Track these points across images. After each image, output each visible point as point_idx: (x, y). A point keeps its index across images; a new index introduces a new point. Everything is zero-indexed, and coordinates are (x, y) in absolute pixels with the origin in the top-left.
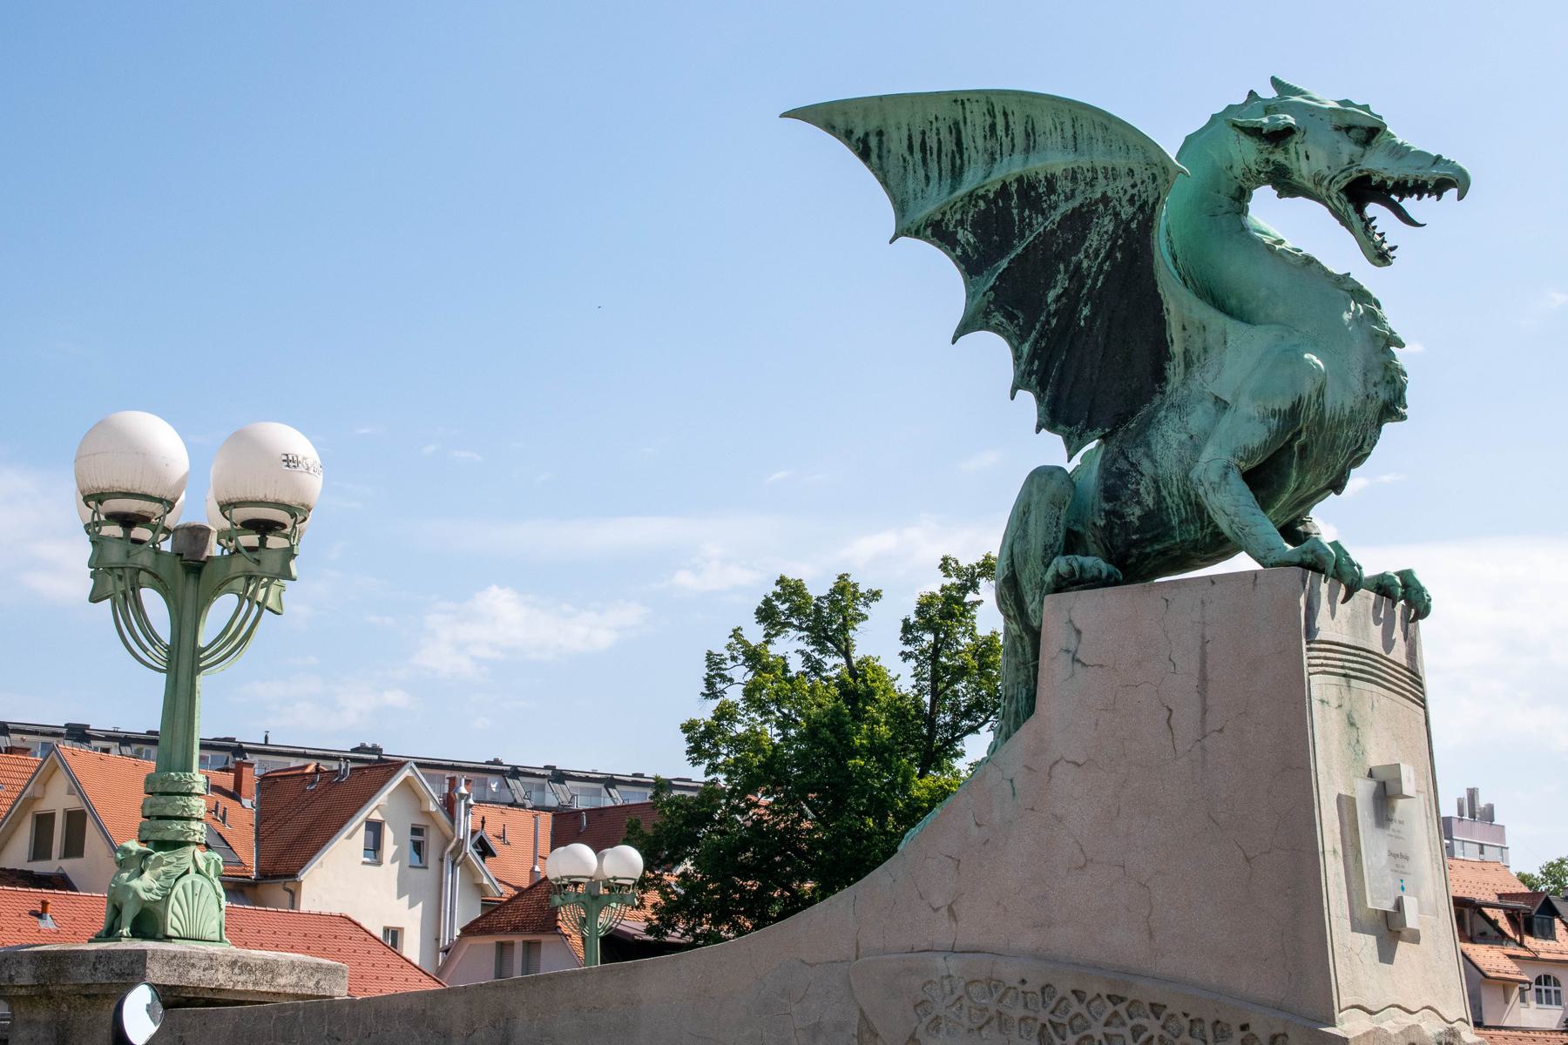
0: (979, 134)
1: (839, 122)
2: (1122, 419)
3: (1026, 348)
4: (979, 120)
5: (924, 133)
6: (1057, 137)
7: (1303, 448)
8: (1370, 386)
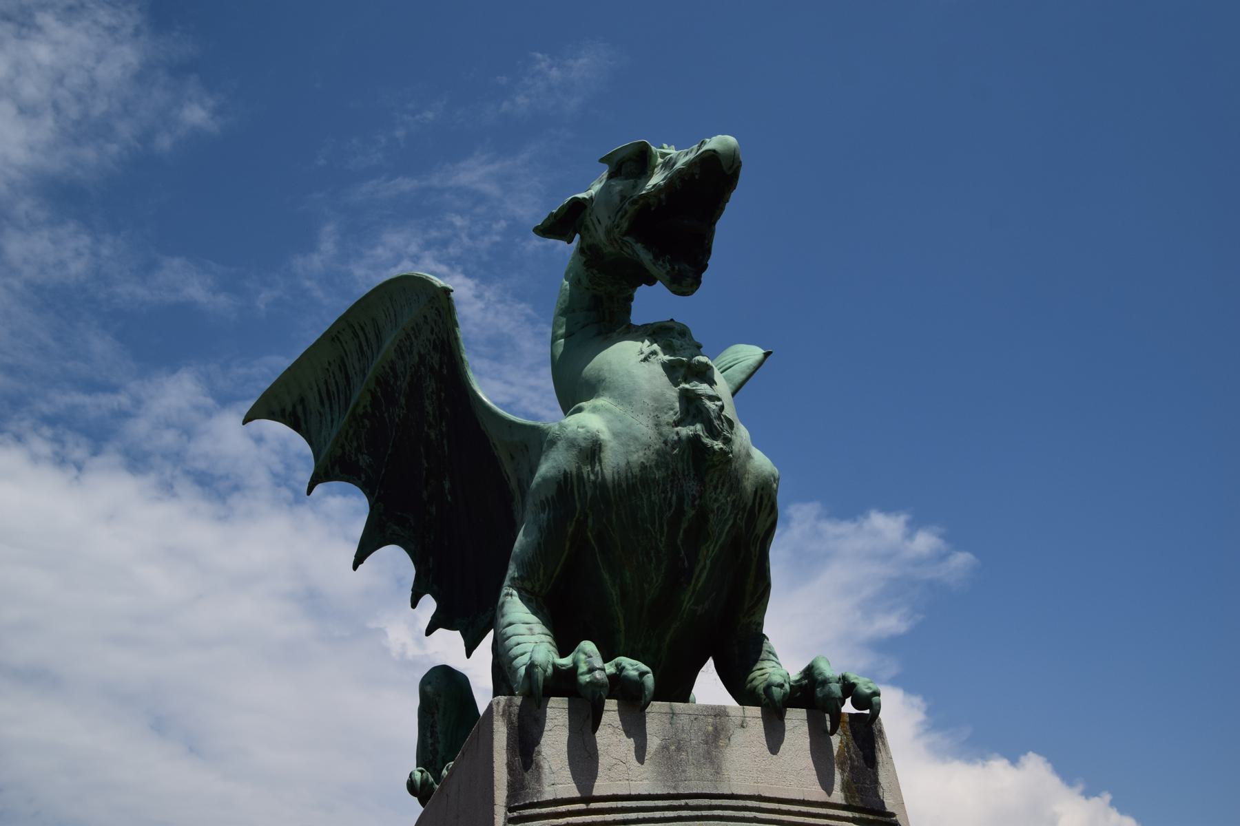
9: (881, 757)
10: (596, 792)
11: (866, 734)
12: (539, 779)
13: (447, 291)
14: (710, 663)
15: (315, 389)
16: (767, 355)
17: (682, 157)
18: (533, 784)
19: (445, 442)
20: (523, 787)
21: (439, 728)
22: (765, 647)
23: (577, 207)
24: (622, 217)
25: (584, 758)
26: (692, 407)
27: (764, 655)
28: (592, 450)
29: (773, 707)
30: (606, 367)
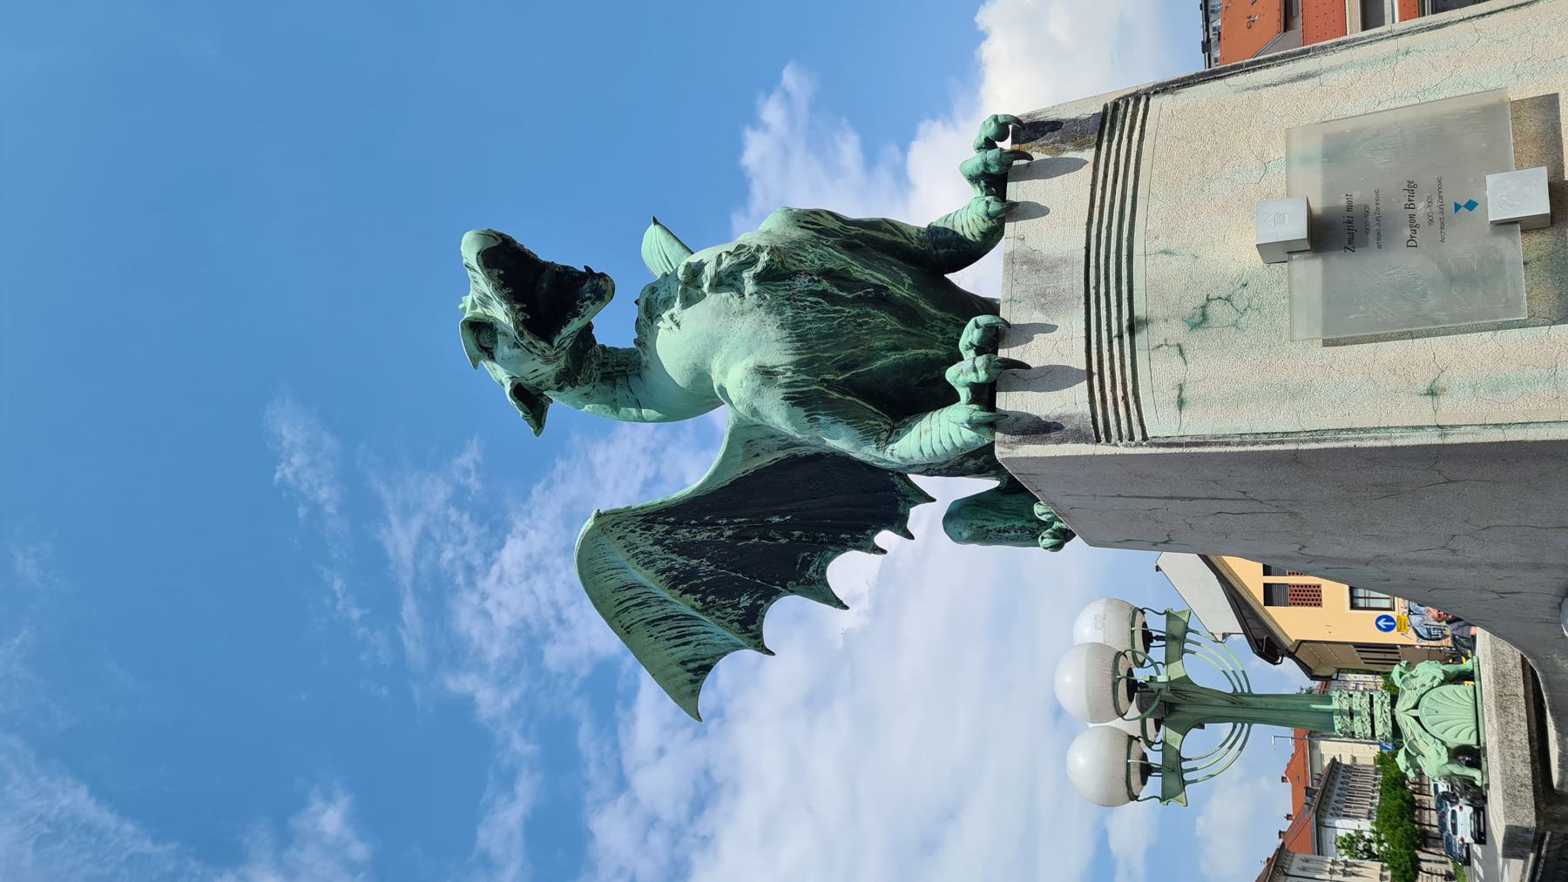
0: (646, 610)
1: (689, 688)
6: (622, 576)
7: (844, 368)
9: (1052, 117)
10: (1084, 367)
11: (1029, 130)
12: (1071, 417)
13: (599, 516)
14: (949, 276)
16: (656, 222)
17: (481, 284)
20: (1078, 430)
21: (1002, 526)
22: (941, 225)
23: (520, 392)
25: (1053, 378)
26: (727, 281)
27: (949, 226)
28: (766, 374)
29: (1004, 214)
30: (682, 363)
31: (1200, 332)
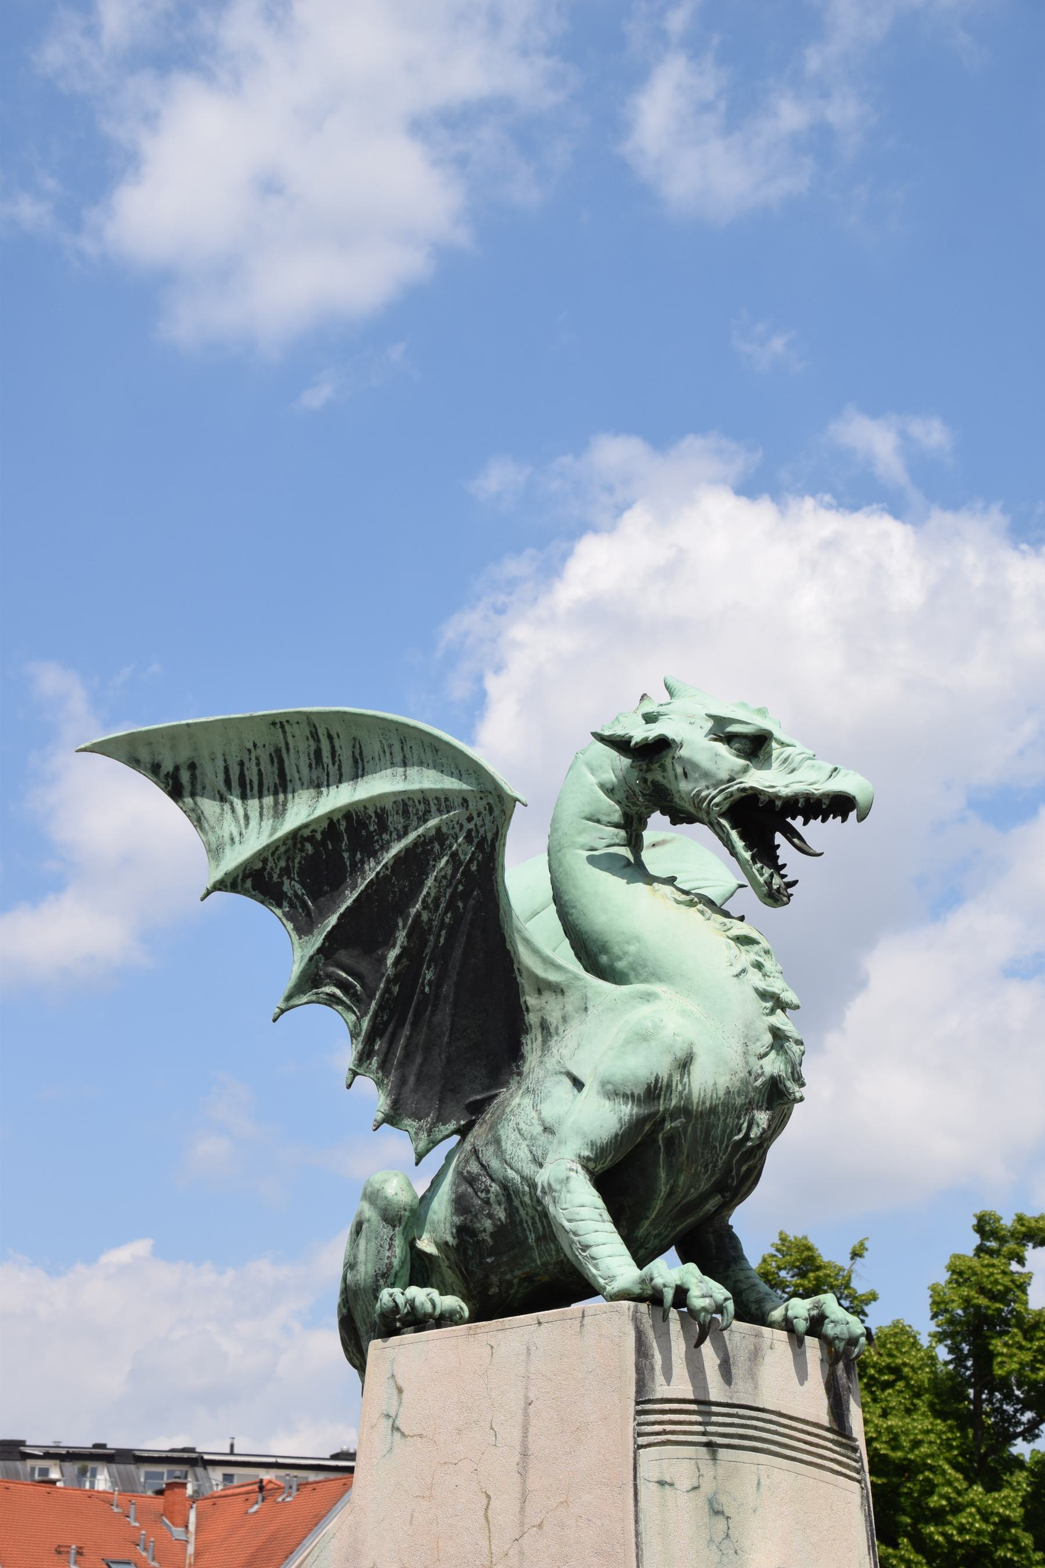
1: (144, 755)
2: (477, 1109)
3: (365, 1024)
4: (302, 745)
5: (242, 764)
8: (753, 1060)
15: (221, 764)
18: (649, 1384)
19: (443, 932)
20: (644, 1386)
24: (725, 799)
31: (707, 1508)
